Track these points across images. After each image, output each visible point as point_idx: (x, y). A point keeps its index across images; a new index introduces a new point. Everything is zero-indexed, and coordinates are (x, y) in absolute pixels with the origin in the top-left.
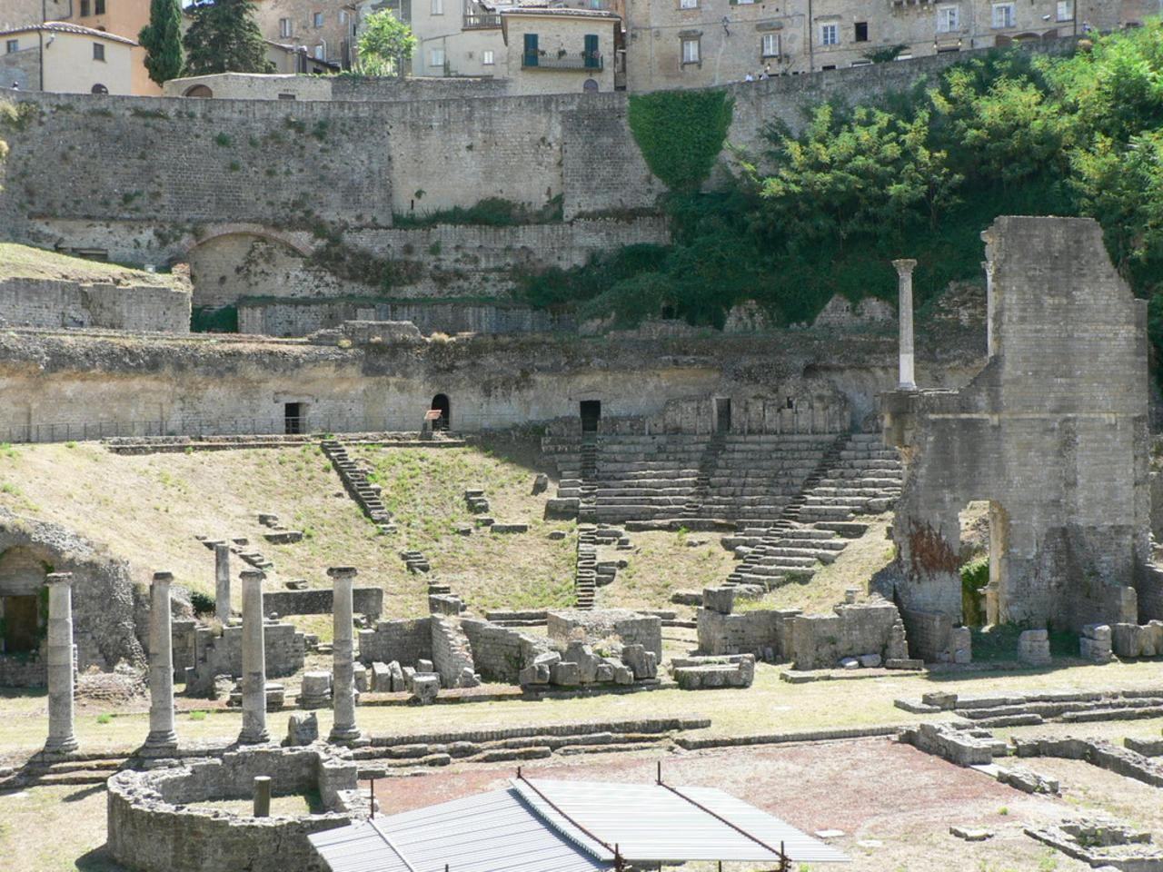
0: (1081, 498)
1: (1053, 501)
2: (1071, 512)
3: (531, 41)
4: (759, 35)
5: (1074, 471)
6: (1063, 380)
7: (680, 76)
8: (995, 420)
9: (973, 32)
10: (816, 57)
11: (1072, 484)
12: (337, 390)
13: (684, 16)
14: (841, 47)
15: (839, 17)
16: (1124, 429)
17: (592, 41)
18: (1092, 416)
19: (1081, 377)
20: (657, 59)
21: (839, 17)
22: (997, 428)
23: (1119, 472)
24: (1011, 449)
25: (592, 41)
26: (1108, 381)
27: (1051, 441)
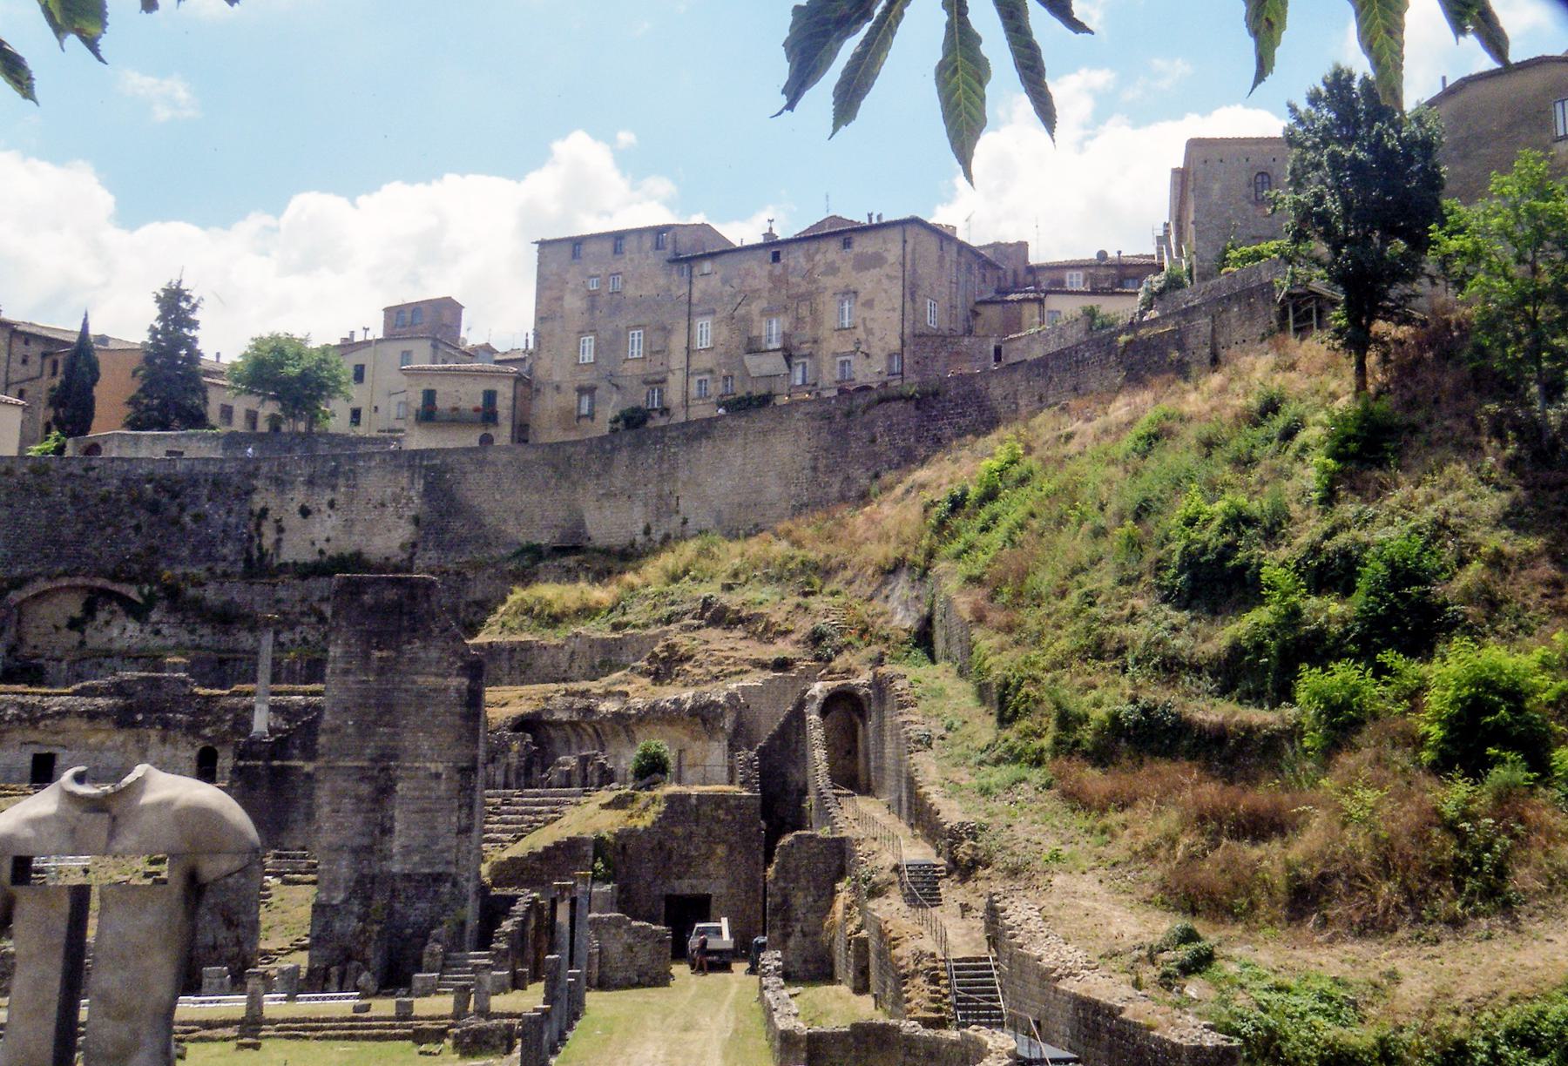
0: (396, 844)
1: (366, 847)
2: (385, 858)
3: (430, 396)
4: (646, 389)
5: (392, 818)
6: (386, 730)
7: (575, 428)
8: (309, 767)
9: (820, 386)
10: (691, 409)
11: (387, 831)
12: (92, 741)
13: (583, 371)
15: (711, 371)
16: (450, 778)
17: (490, 396)
18: (417, 765)
19: (405, 727)
20: (556, 413)
22: (309, 776)
23: (440, 820)
24: (323, 795)
25: (490, 396)
26: (436, 730)
27: (365, 789)
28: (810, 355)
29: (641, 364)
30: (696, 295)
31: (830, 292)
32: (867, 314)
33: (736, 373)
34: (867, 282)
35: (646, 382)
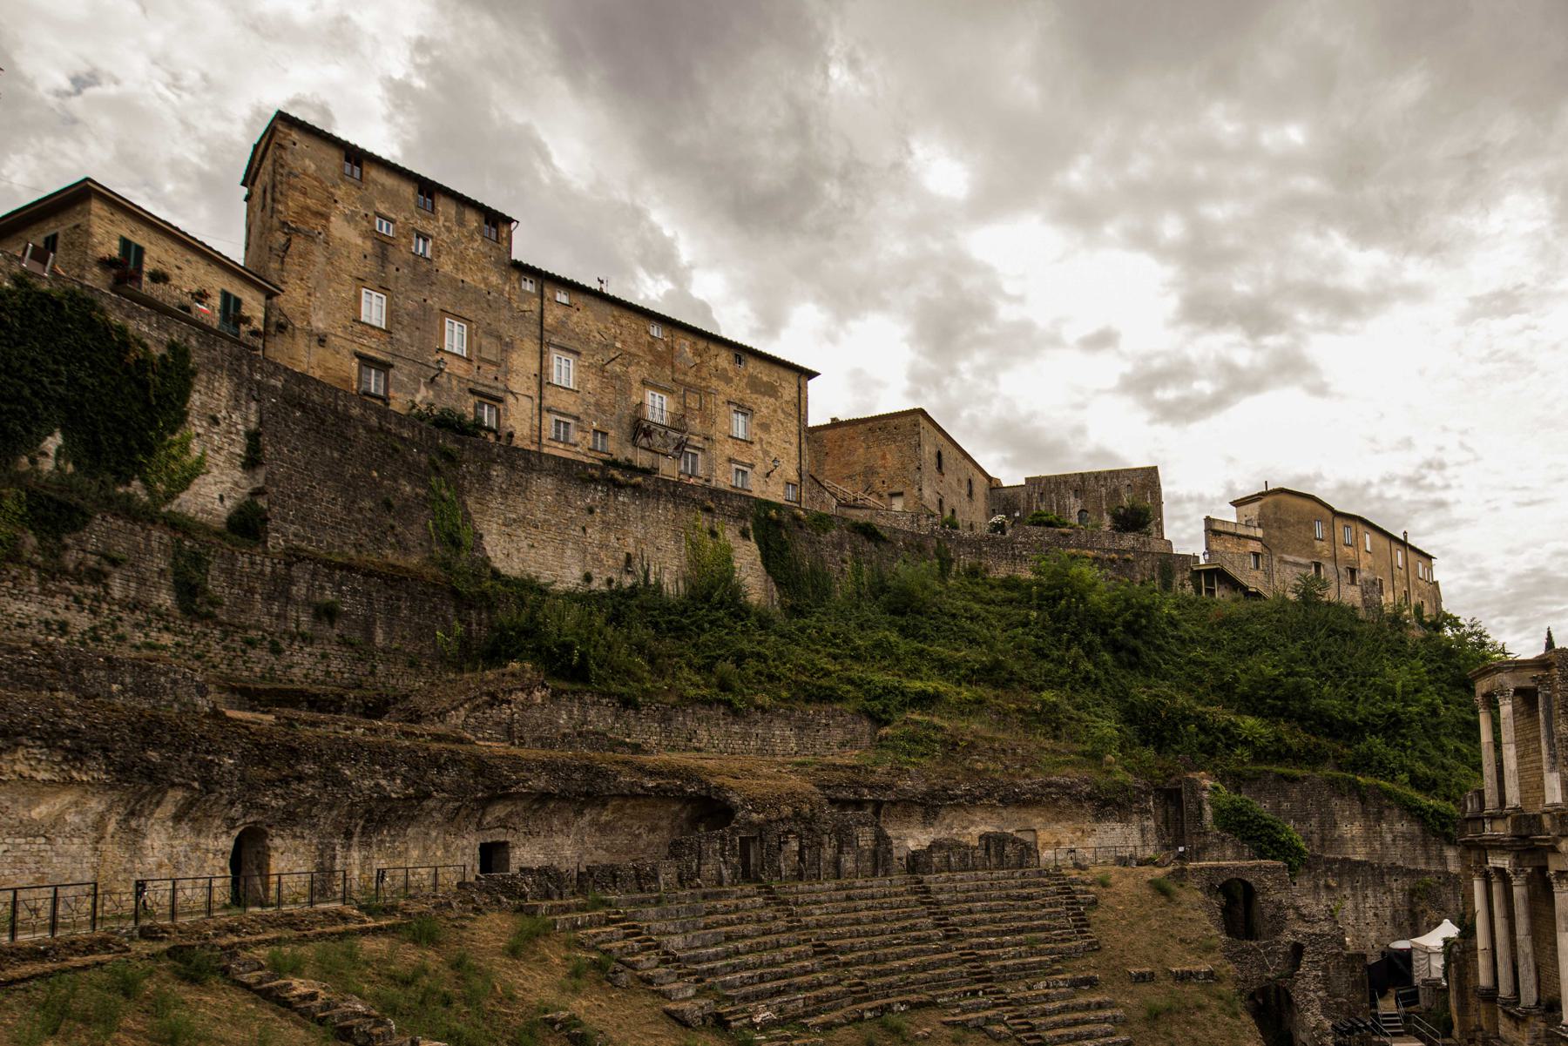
4: (473, 400)
14: (578, 449)
15: (577, 418)
21: (577, 418)
28: (703, 450)
29: (464, 365)
30: (549, 320)
31: (722, 398)
32: (765, 437)
33: (612, 433)
34: (764, 405)
35: (472, 391)
